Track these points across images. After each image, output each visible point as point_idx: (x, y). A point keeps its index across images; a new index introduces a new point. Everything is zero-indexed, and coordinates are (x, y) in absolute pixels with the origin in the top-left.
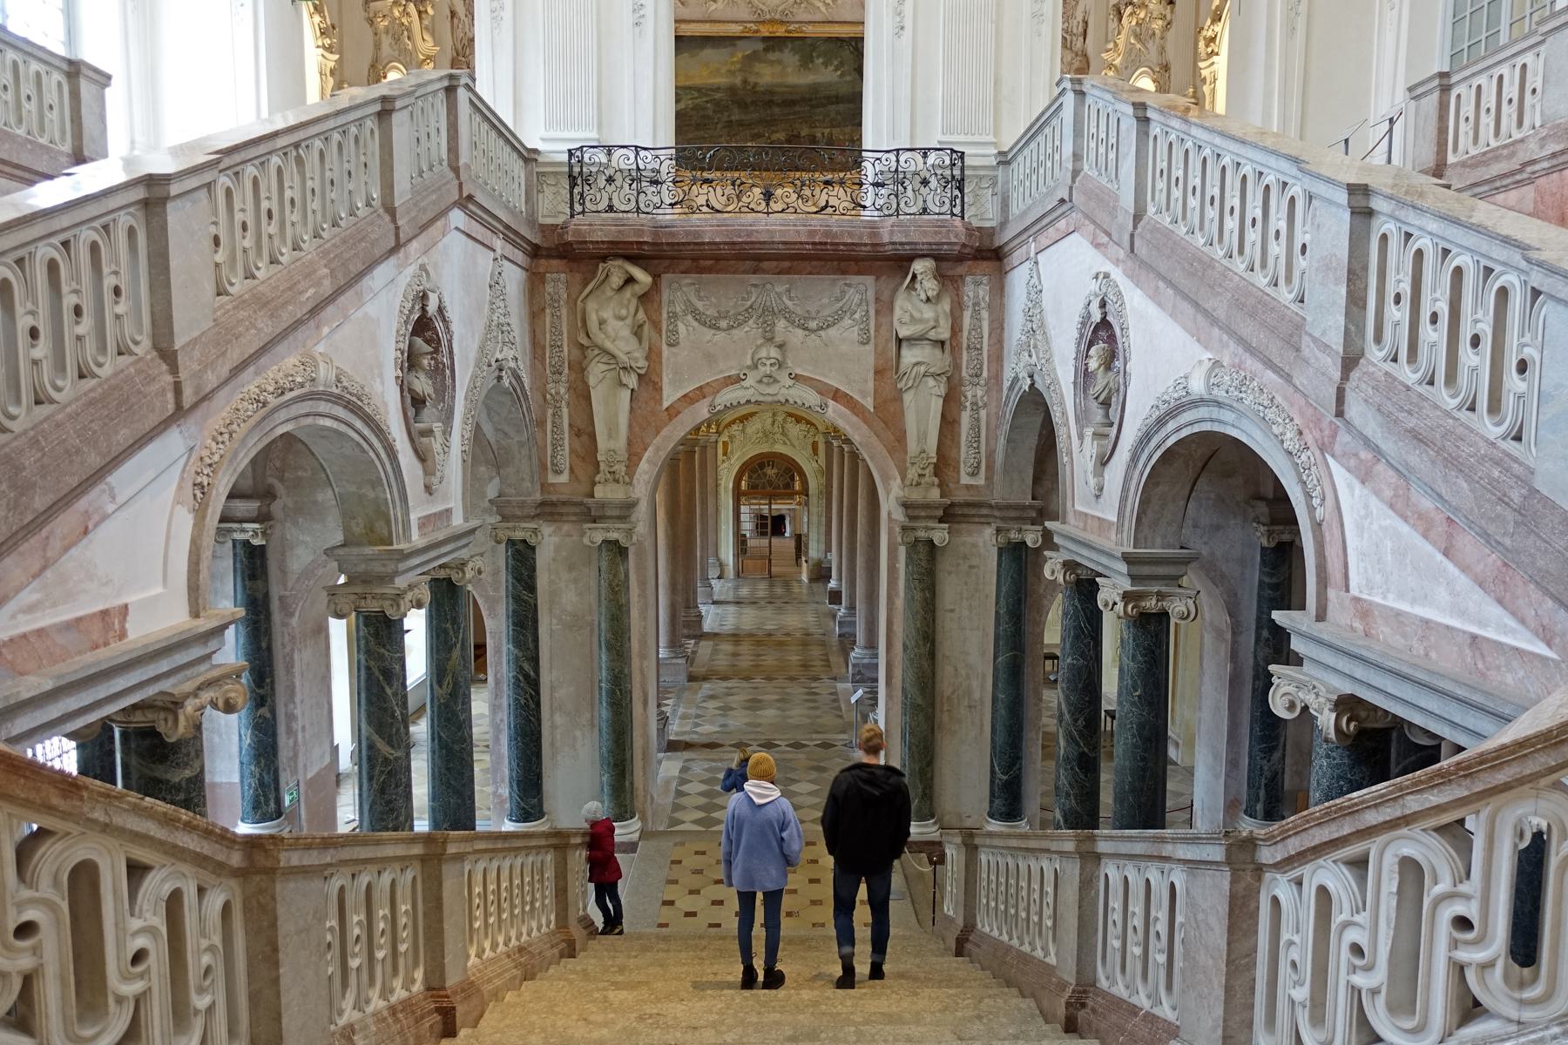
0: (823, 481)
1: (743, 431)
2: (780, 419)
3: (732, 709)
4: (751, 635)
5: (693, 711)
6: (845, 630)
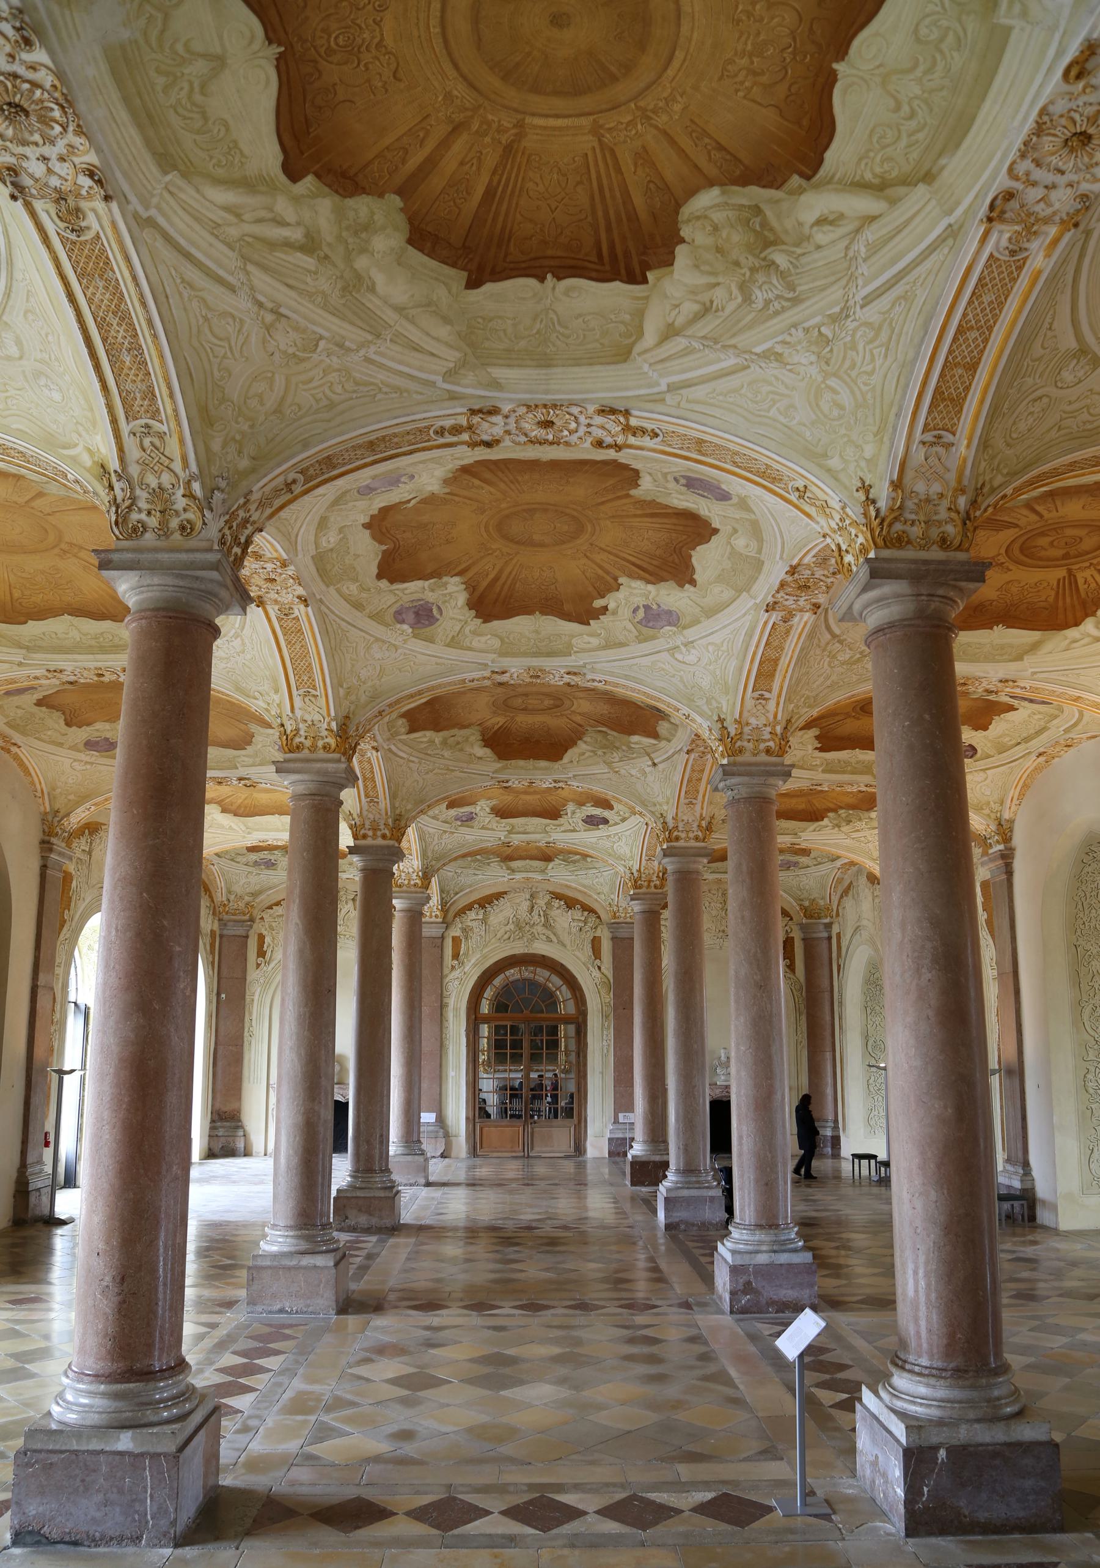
0: (609, 998)
1: (484, 921)
2: (541, 902)
3: (435, 1382)
4: (493, 1229)
5: (325, 1389)
6: (680, 1215)
